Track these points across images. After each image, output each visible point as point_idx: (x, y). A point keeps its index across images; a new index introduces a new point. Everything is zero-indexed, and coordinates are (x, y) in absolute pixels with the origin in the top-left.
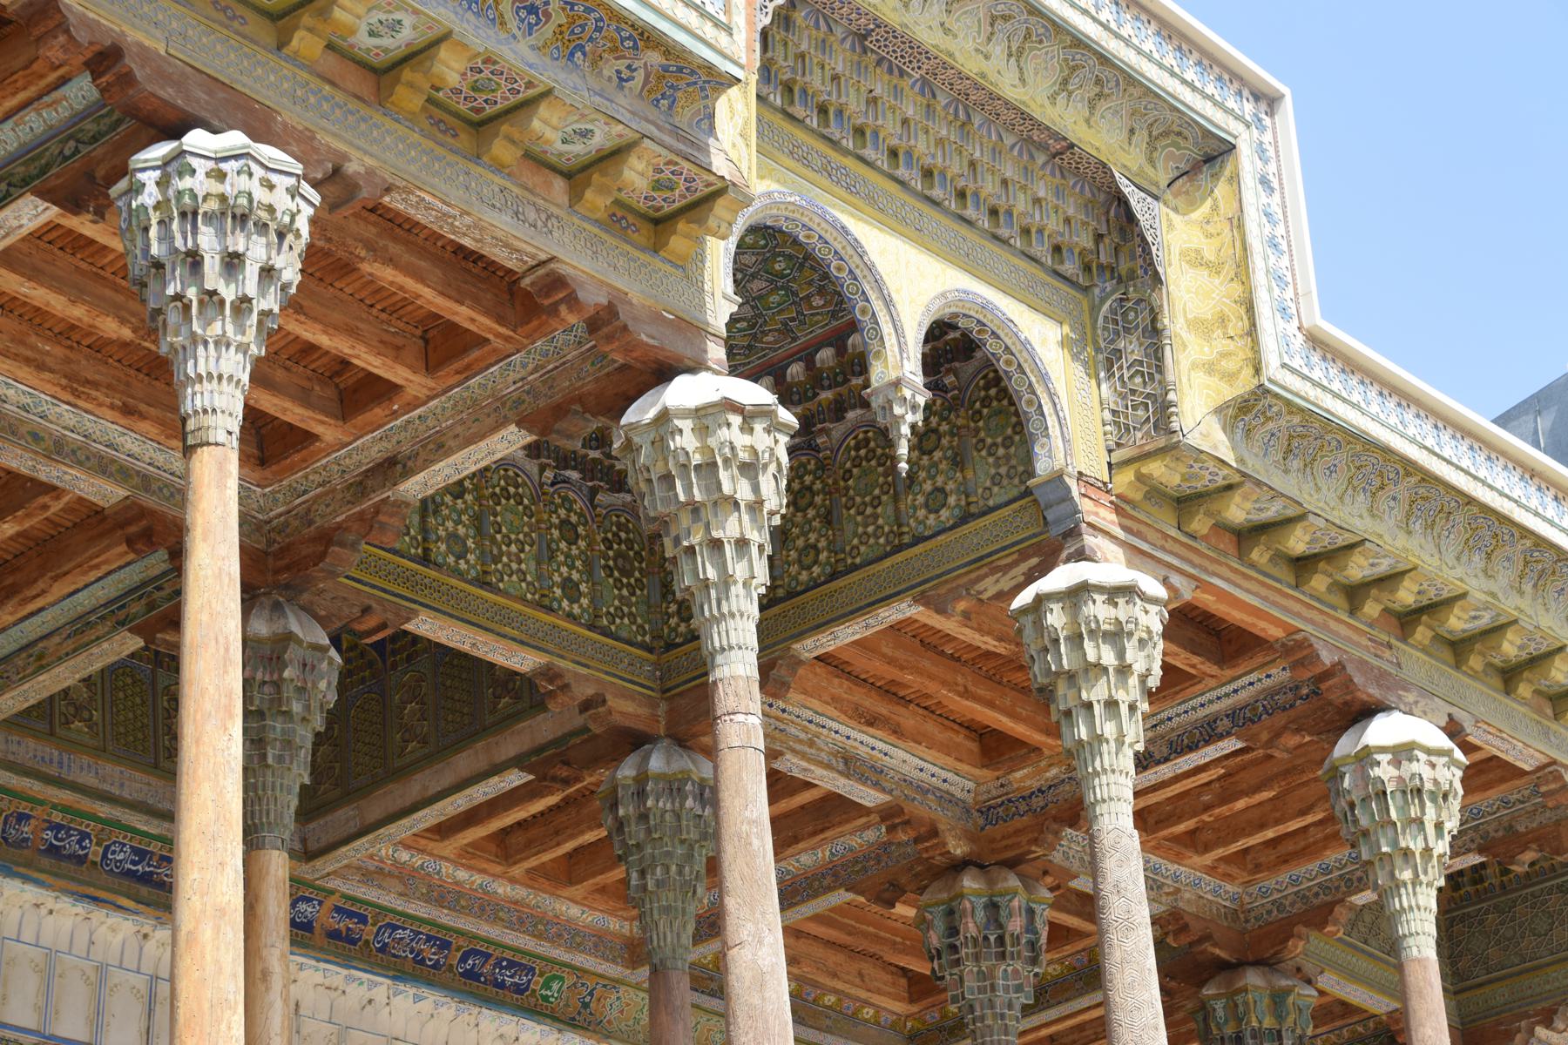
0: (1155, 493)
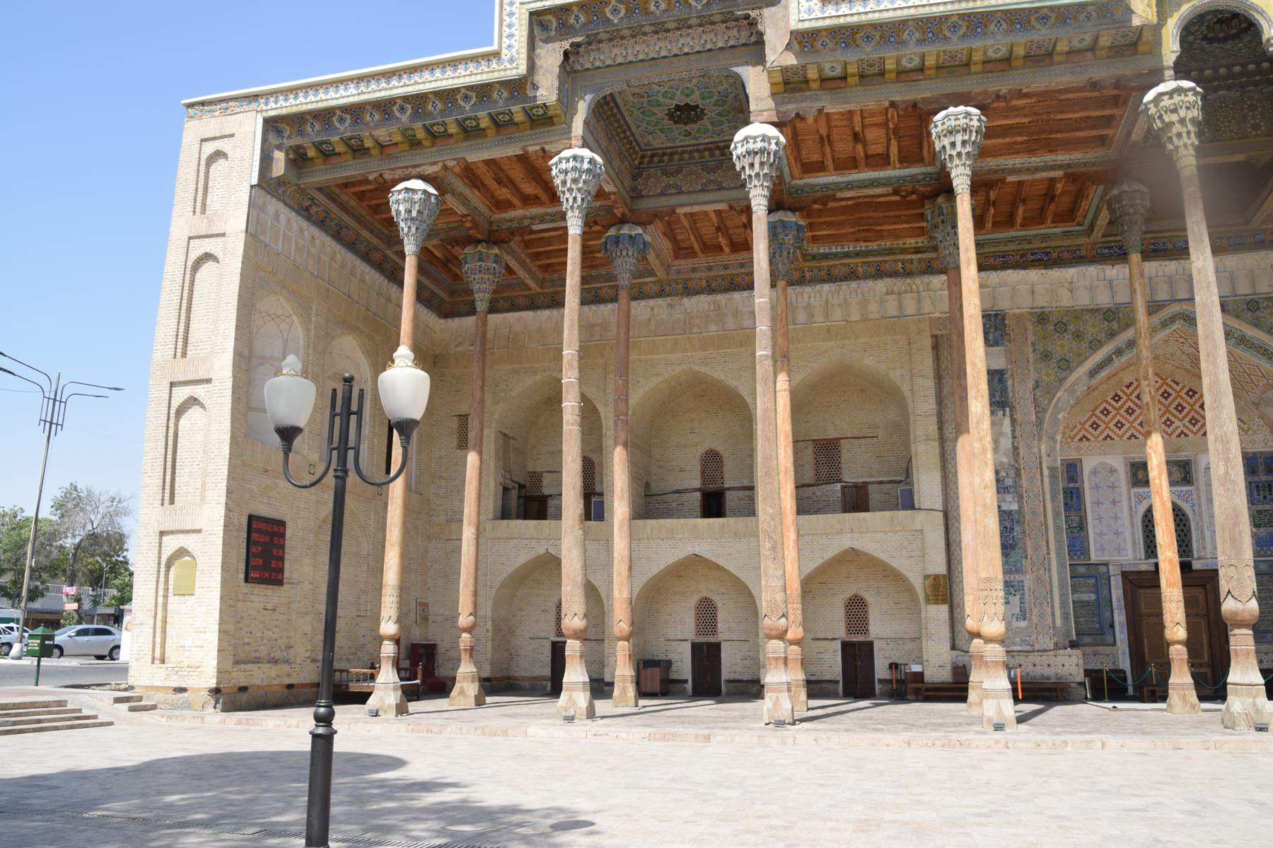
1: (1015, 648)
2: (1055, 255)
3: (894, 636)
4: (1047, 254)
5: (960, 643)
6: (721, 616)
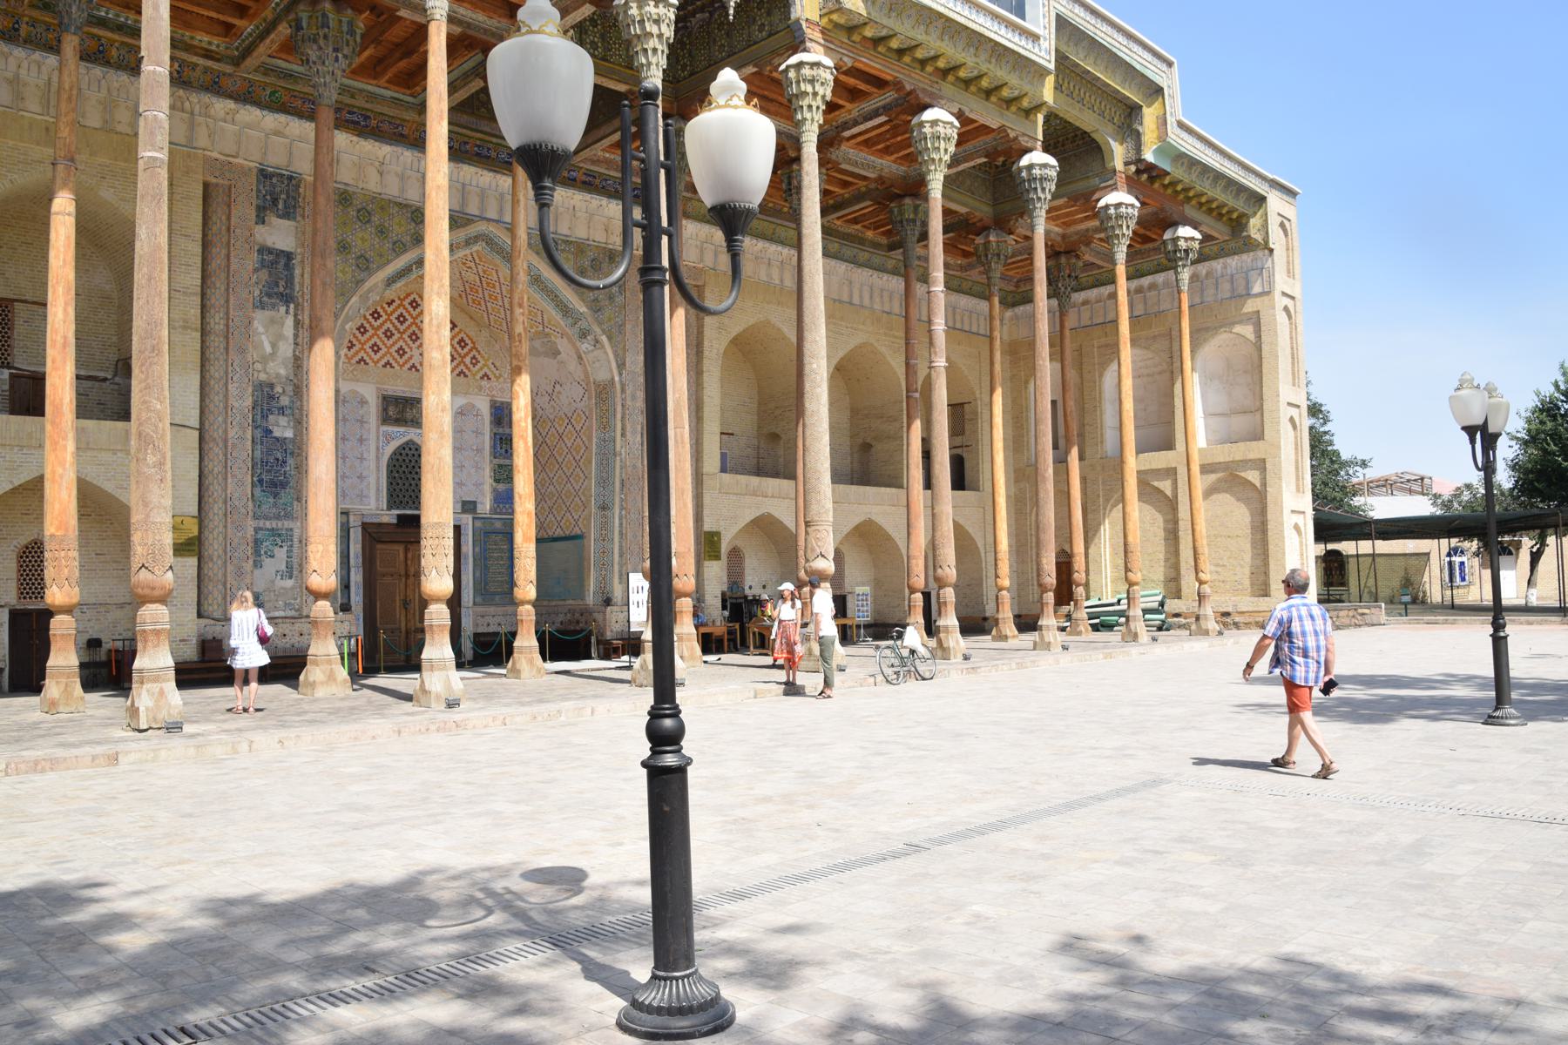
0: (837, 25)
1: (277, 614)
2: (374, 123)
3: (92, 600)
4: (366, 118)
5: (213, 608)
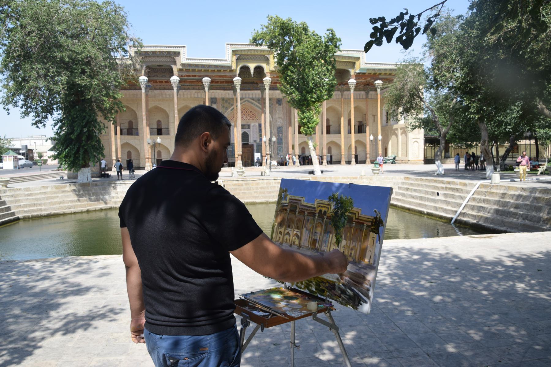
6: (162, 154)
